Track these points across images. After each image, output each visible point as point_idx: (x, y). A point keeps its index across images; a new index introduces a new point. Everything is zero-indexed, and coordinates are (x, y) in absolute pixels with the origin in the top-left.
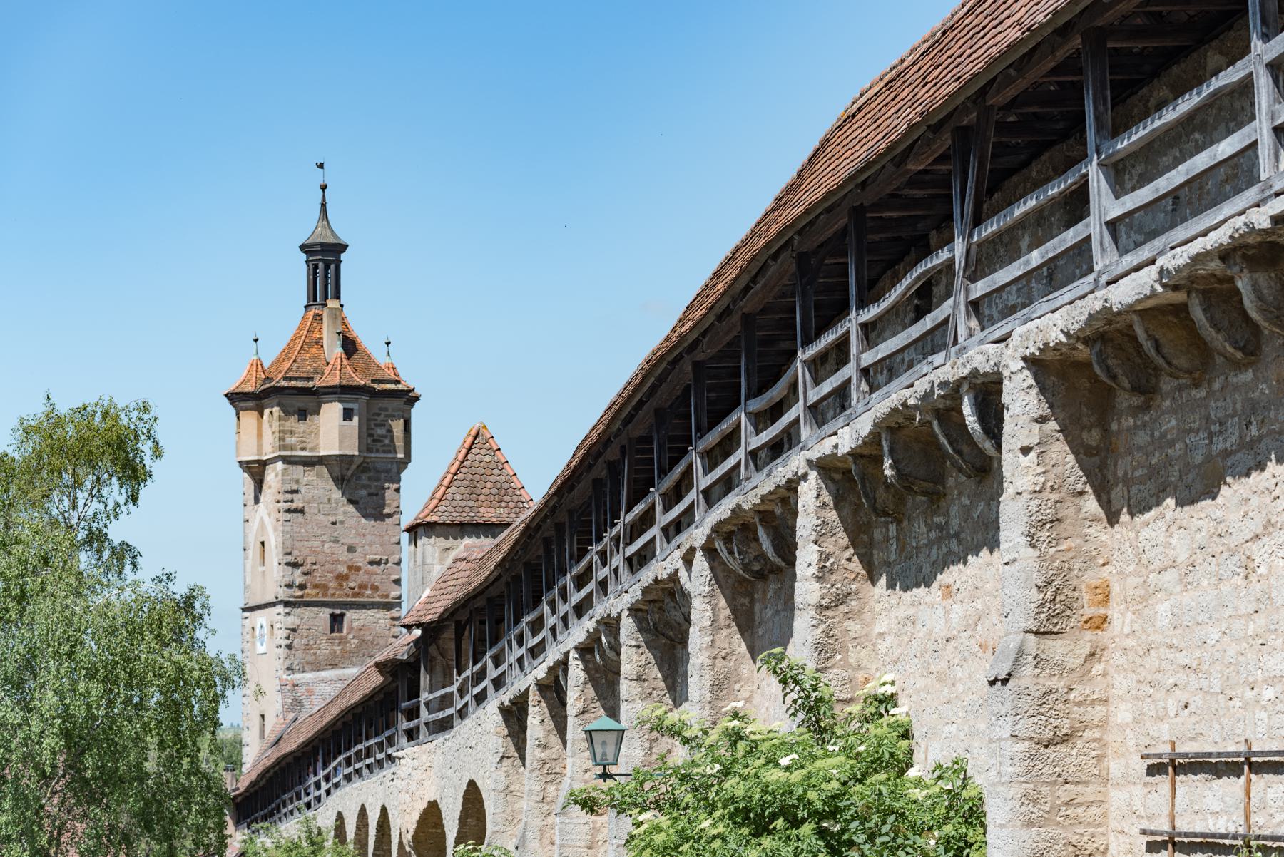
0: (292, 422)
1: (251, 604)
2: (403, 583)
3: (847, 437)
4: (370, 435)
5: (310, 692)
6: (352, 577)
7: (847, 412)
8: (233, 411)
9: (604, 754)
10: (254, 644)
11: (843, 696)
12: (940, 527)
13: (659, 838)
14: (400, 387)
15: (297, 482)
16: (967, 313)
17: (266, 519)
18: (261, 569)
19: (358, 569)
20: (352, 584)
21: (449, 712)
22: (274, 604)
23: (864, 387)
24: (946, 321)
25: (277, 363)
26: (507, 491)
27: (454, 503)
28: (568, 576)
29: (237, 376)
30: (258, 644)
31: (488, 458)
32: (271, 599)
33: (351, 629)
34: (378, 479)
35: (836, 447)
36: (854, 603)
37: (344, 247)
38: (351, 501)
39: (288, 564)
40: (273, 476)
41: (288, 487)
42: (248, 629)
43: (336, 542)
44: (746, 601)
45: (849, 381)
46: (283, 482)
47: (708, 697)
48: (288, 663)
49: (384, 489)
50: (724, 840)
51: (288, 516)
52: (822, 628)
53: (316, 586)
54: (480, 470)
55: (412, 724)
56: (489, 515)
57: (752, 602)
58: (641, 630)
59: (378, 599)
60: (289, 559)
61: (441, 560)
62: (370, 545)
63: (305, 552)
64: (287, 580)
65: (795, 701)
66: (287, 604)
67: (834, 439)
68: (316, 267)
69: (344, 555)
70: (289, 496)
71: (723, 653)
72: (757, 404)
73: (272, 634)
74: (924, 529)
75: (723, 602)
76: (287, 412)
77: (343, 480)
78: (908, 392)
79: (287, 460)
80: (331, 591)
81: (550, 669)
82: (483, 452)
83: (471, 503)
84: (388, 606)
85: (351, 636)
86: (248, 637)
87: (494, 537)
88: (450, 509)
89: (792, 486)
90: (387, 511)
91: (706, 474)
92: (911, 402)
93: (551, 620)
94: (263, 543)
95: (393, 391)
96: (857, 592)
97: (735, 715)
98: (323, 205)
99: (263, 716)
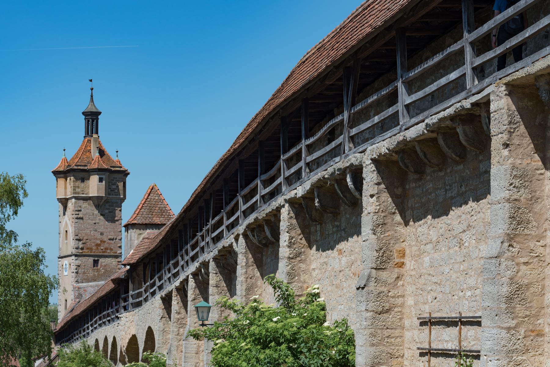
0: (79, 183)
1: (62, 255)
2: (122, 247)
3: (300, 190)
4: (110, 188)
6: (102, 245)
7: (301, 180)
8: (55, 178)
9: (203, 316)
11: (298, 294)
12: (337, 226)
13: (225, 350)
14: (122, 169)
15: (80, 207)
16: (349, 141)
17: (68, 222)
18: (66, 241)
19: (105, 242)
20: (102, 248)
21: (140, 299)
22: (71, 256)
23: (308, 170)
24: (340, 144)
25: (73, 159)
26: (164, 211)
27: (143, 216)
28: (189, 245)
29: (57, 165)
31: (157, 198)
32: (70, 253)
33: (101, 266)
34: (113, 206)
35: (296, 194)
36: (303, 256)
37: (100, 113)
38: (102, 215)
39: (77, 240)
40: (71, 204)
41: (77, 209)
42: (61, 265)
43: (96, 231)
44: (260, 255)
45: (301, 167)
46: (75, 207)
47: (244, 293)
49: (115, 210)
50: (250, 351)
51: (77, 220)
52: (290, 266)
53: (88, 249)
54: (154, 203)
55: (126, 304)
56: (157, 221)
57: (262, 256)
58: (217, 267)
59: (112, 254)
60: (77, 237)
61: (138, 238)
62: (109, 232)
63: (83, 235)
64: (76, 246)
65: (279, 296)
66: (76, 256)
67: (295, 191)
68: (88, 121)
69: (99, 236)
70: (77, 213)
71: (250, 276)
72: (264, 177)
74: (331, 227)
75: (250, 256)
76: (77, 179)
77: (99, 206)
78: (325, 173)
79: (76, 198)
81: (181, 282)
82: (155, 195)
83: (150, 216)
84: (117, 257)
86: (60, 269)
87: (159, 229)
88: (141, 218)
89: (278, 210)
90: (116, 219)
91: (244, 204)
92: (326, 176)
93: (182, 263)
94: (66, 231)
95: (119, 171)
96: (304, 252)
97: (255, 301)
98: (92, 96)
99: (66, 300)
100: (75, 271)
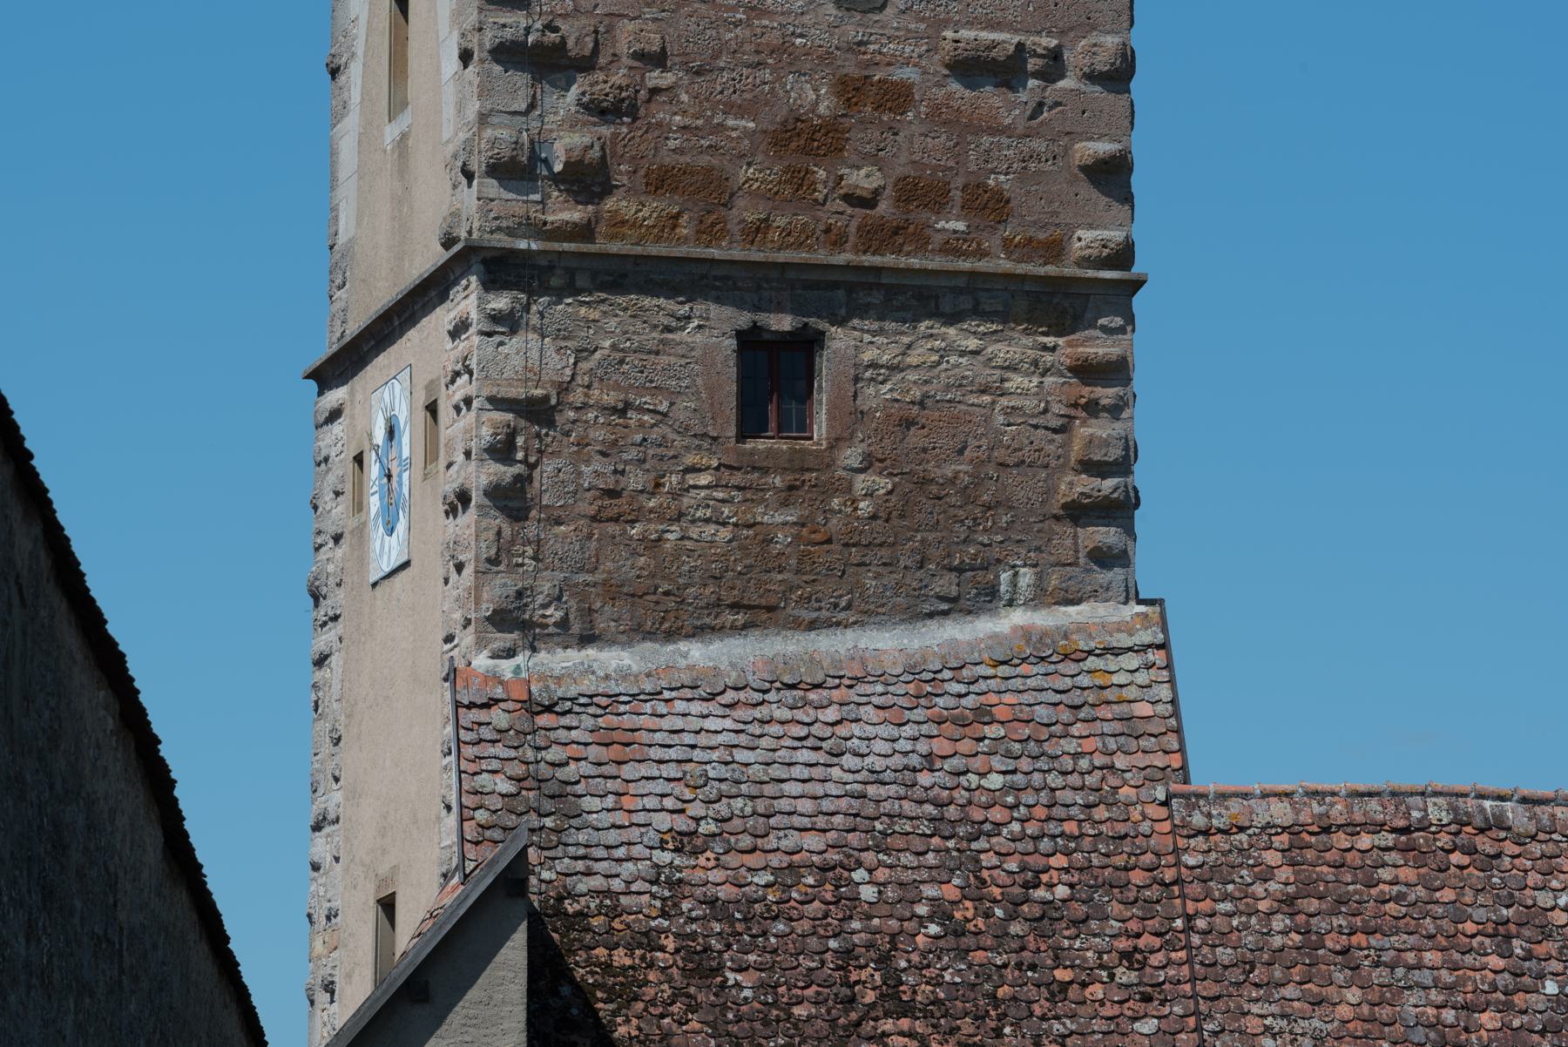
5: (622, 743)
6: (861, 139)
10: (361, 532)
19: (897, 97)
20: (862, 179)
30: (377, 534)
32: (428, 257)
33: (851, 419)
39: (508, 54)
42: (342, 466)
48: (499, 588)
59: (1004, 264)
64: (503, 133)
73: (431, 454)
80: (746, 211)
85: (851, 456)
86: (337, 513)
99: (388, 906)
100: (482, 475)
